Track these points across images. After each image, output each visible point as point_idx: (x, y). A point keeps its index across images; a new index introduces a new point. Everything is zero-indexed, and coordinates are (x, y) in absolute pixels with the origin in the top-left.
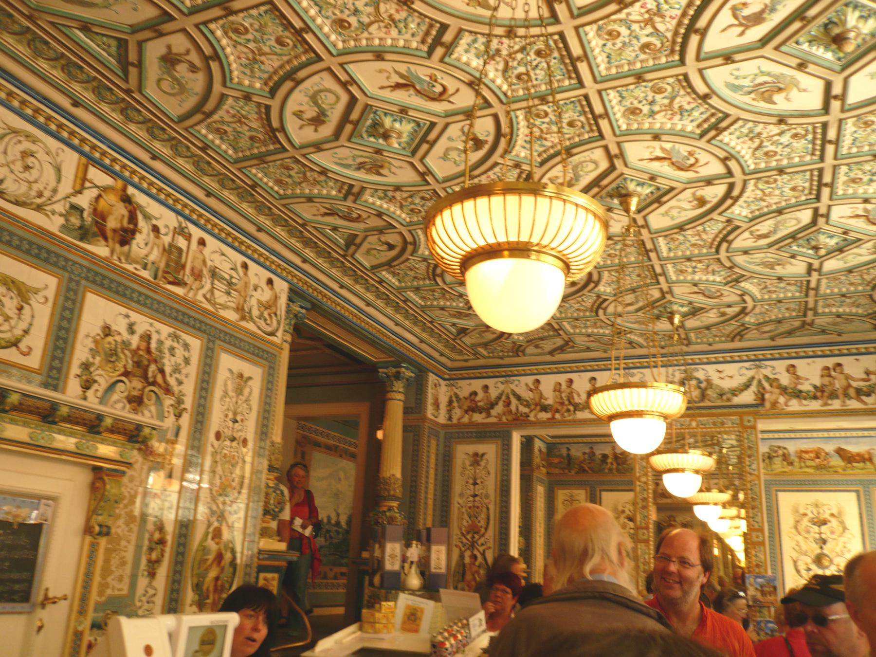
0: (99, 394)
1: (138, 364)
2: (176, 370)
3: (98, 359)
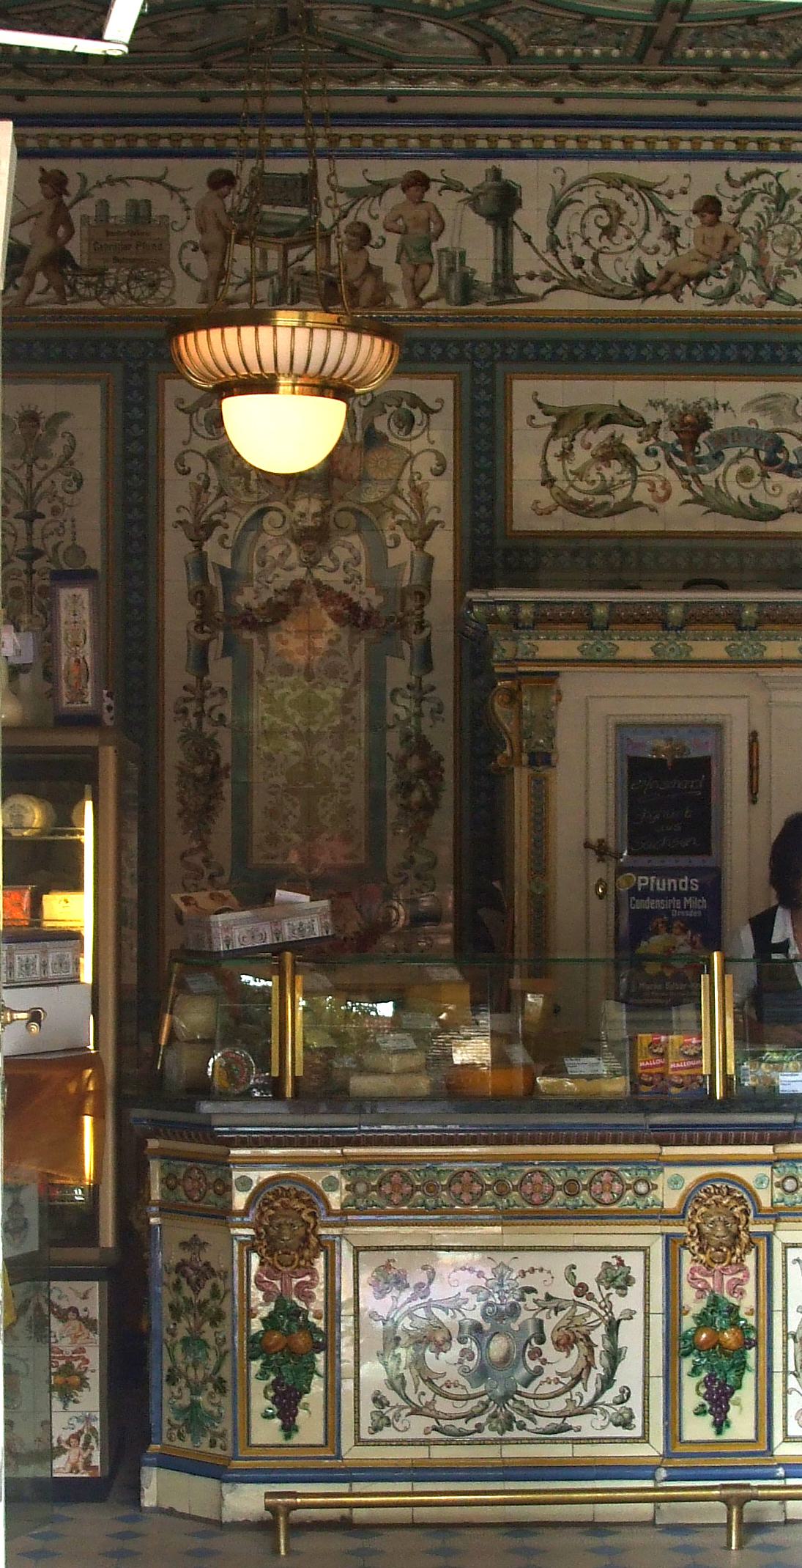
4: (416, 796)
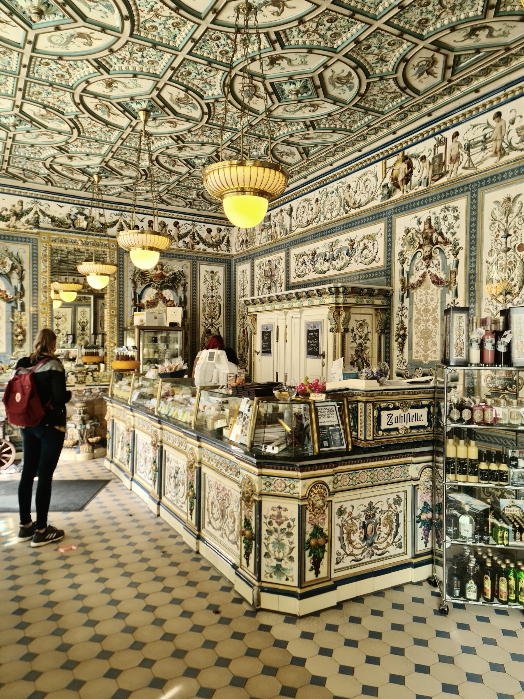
0: (409, 264)
1: (426, 238)
2: (451, 227)
3: (406, 247)
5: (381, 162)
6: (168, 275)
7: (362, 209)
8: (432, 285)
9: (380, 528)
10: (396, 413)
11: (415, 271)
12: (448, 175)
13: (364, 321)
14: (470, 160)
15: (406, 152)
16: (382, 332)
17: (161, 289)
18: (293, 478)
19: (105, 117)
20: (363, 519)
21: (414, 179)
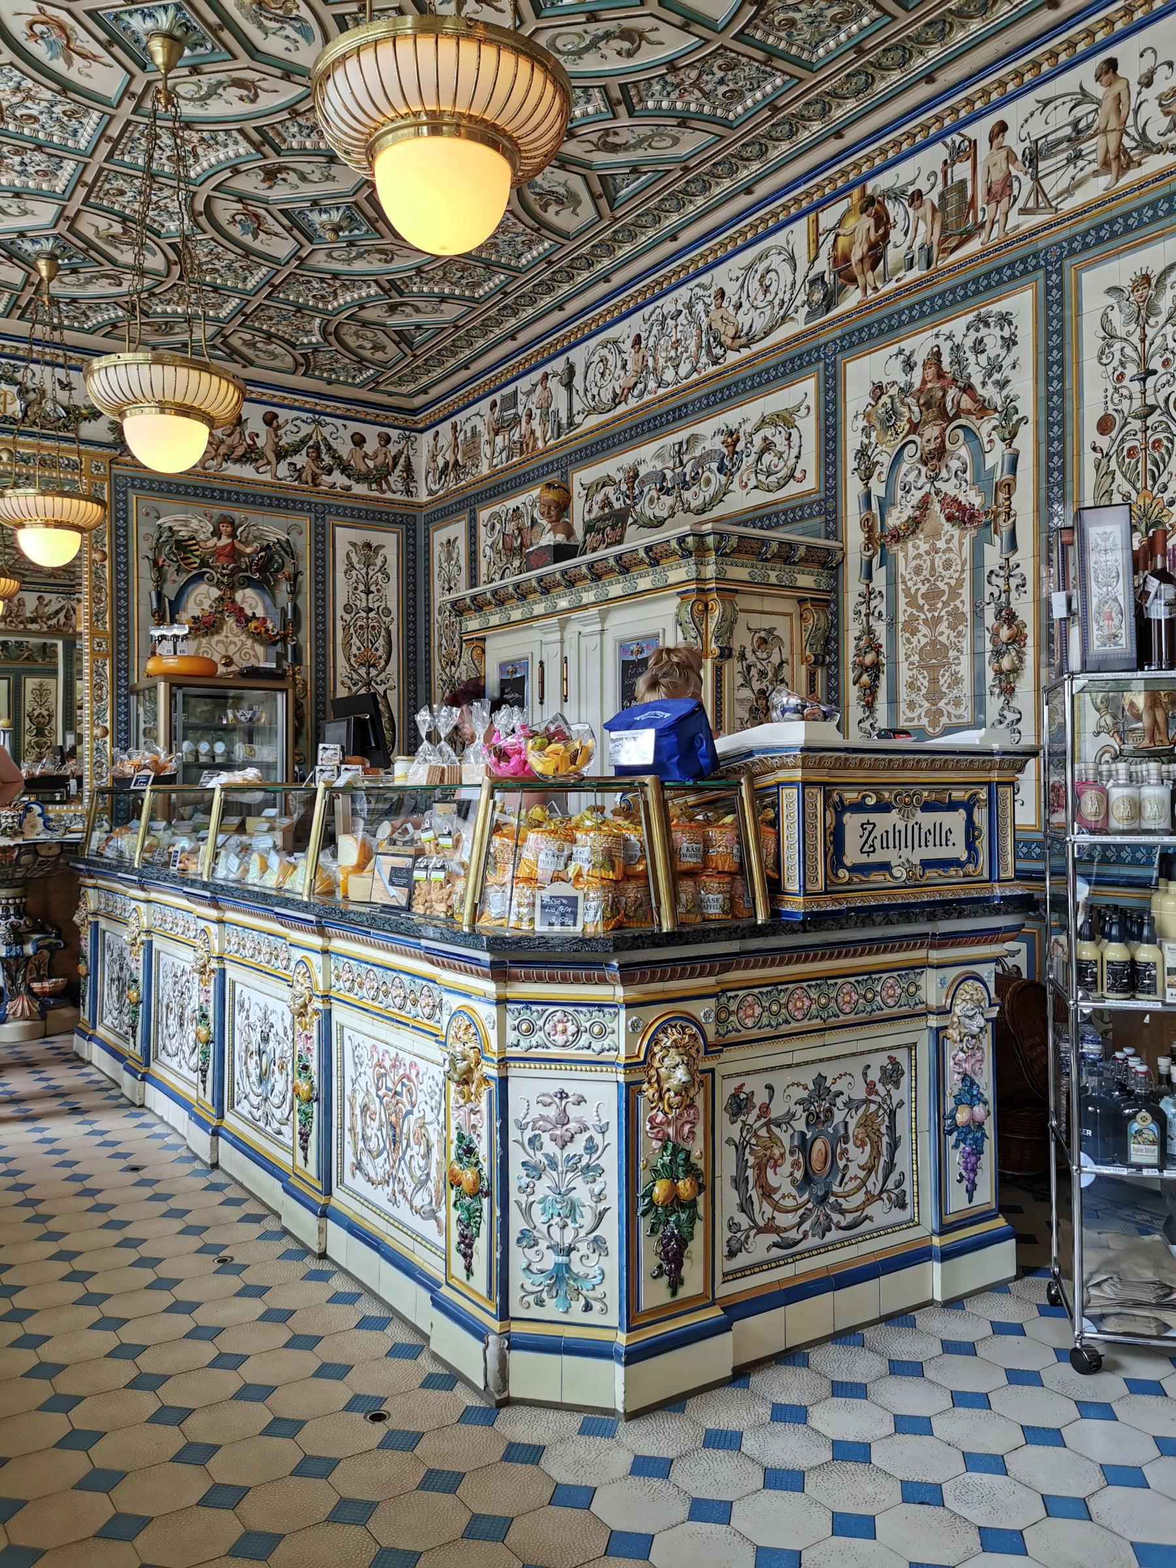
0: (884, 477)
1: (928, 405)
2: (994, 366)
3: (874, 434)
4: (1006, 663)
5: (805, 219)
6: (249, 550)
7: (756, 348)
8: (947, 526)
9: (846, 1151)
10: (886, 821)
11: (900, 493)
12: (984, 234)
13: (770, 631)
14: (1038, 190)
15: (870, 185)
16: (818, 662)
17: (232, 588)
18: (601, 1006)
19: (59, 65)
20: (800, 1125)
21: (893, 256)
